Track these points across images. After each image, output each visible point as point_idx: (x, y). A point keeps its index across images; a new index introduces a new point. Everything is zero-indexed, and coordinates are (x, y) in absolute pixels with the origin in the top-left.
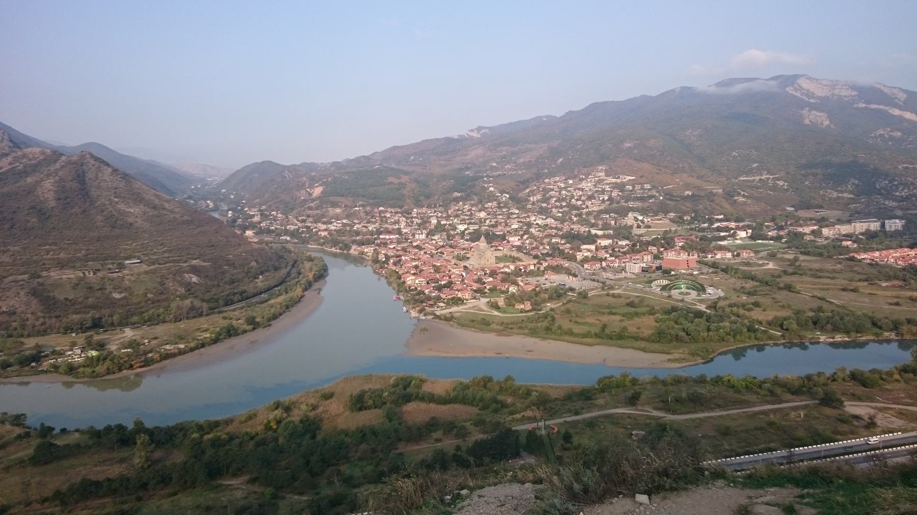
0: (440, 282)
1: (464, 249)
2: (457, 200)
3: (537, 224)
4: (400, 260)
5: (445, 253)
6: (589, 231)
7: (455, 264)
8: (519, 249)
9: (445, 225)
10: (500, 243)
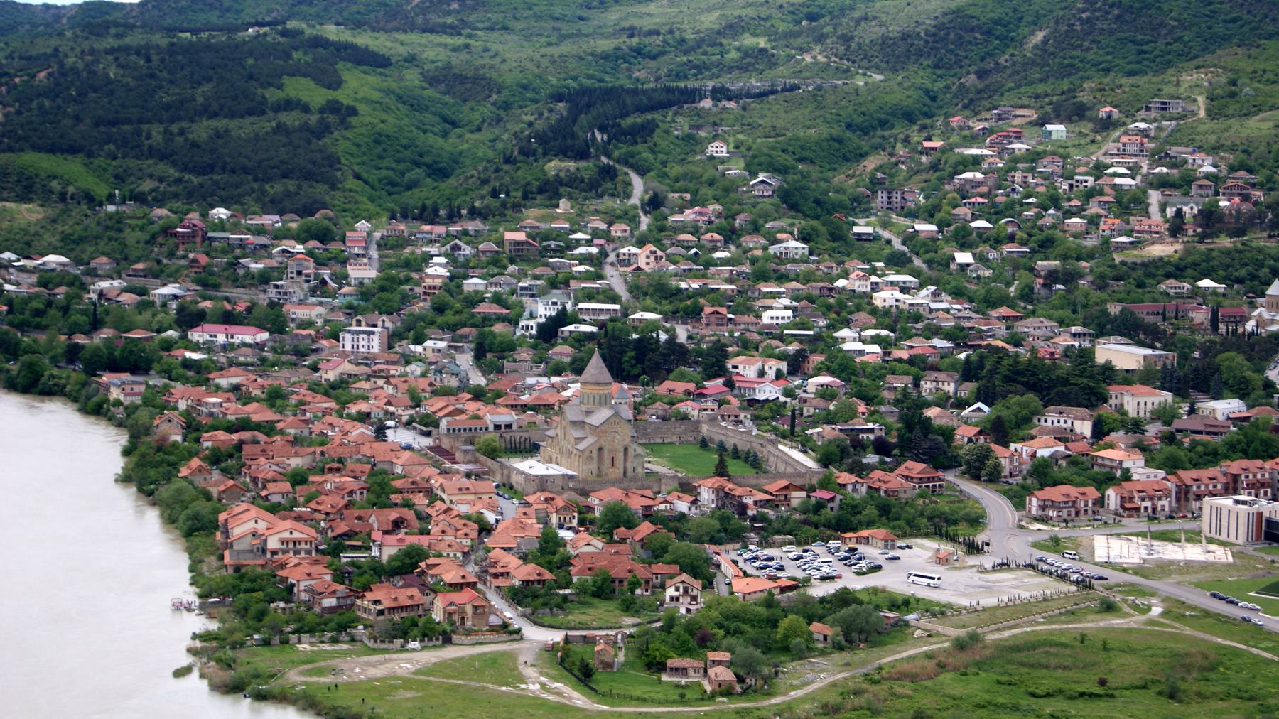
0: (375, 552)
1: (524, 408)
2: (550, 191)
3: (874, 311)
5: (443, 424)
6: (1085, 356)
7: (468, 475)
8: (763, 412)
9: (475, 299)
10: (692, 387)
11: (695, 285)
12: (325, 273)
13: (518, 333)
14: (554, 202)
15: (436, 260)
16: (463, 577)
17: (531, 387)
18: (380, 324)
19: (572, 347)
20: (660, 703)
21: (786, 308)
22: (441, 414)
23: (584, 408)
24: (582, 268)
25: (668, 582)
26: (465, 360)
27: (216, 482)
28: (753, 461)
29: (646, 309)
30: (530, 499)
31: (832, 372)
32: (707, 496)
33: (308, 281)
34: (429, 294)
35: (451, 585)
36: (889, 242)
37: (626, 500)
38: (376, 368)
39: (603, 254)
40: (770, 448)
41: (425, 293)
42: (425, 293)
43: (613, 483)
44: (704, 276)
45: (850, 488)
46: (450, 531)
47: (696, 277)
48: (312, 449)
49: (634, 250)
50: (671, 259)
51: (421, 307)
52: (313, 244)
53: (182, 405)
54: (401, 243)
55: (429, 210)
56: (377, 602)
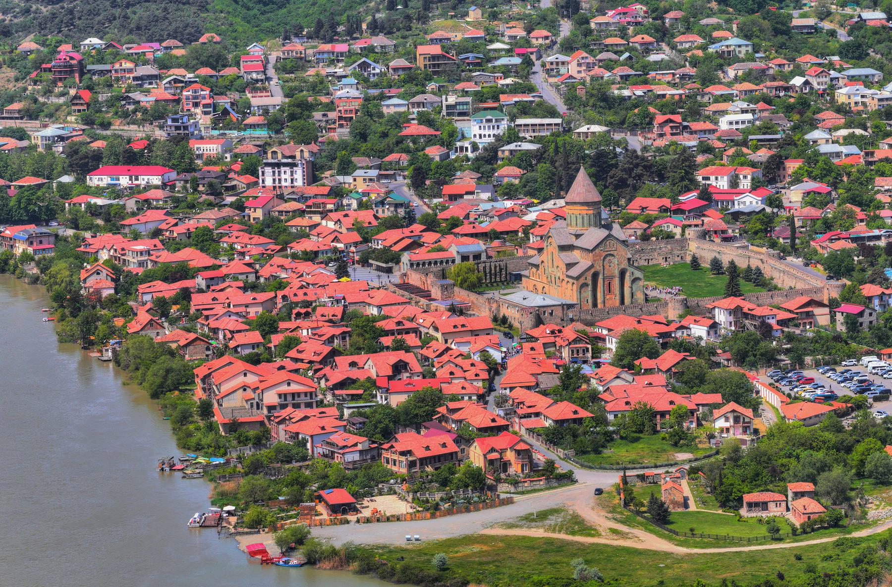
3: (841, 110)
4: (185, 295)
5: (405, 258)
9: (398, 121)
11: (639, 93)
12: (224, 102)
13: (453, 157)
14: (461, 9)
15: (344, 81)
16: (493, 420)
17: (486, 213)
18: (298, 155)
19: (519, 167)
20: (750, 542)
21: (744, 111)
22: (396, 248)
23: (573, 230)
24: (509, 81)
25: (717, 413)
26: (403, 189)
27: (169, 334)
28: (757, 278)
29: (591, 122)
30: (535, 333)
31: (814, 179)
32: (721, 317)
33: (206, 113)
34: (345, 119)
35: (480, 430)
36: (833, 33)
37: (638, 326)
38: (310, 203)
39: (528, 63)
40: (772, 262)
41: (340, 118)
42: (340, 118)
43: (616, 311)
44: (646, 82)
45: (876, 302)
46: (458, 372)
47: (635, 84)
48: (272, 294)
49: (562, 58)
50: (609, 66)
51: (342, 133)
52: (205, 71)
53: (104, 256)
54: (300, 63)
55: (326, 27)
56: (409, 452)
